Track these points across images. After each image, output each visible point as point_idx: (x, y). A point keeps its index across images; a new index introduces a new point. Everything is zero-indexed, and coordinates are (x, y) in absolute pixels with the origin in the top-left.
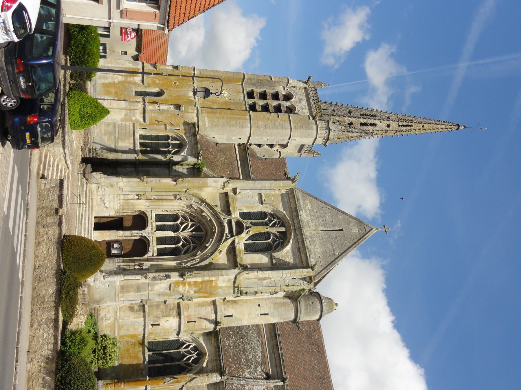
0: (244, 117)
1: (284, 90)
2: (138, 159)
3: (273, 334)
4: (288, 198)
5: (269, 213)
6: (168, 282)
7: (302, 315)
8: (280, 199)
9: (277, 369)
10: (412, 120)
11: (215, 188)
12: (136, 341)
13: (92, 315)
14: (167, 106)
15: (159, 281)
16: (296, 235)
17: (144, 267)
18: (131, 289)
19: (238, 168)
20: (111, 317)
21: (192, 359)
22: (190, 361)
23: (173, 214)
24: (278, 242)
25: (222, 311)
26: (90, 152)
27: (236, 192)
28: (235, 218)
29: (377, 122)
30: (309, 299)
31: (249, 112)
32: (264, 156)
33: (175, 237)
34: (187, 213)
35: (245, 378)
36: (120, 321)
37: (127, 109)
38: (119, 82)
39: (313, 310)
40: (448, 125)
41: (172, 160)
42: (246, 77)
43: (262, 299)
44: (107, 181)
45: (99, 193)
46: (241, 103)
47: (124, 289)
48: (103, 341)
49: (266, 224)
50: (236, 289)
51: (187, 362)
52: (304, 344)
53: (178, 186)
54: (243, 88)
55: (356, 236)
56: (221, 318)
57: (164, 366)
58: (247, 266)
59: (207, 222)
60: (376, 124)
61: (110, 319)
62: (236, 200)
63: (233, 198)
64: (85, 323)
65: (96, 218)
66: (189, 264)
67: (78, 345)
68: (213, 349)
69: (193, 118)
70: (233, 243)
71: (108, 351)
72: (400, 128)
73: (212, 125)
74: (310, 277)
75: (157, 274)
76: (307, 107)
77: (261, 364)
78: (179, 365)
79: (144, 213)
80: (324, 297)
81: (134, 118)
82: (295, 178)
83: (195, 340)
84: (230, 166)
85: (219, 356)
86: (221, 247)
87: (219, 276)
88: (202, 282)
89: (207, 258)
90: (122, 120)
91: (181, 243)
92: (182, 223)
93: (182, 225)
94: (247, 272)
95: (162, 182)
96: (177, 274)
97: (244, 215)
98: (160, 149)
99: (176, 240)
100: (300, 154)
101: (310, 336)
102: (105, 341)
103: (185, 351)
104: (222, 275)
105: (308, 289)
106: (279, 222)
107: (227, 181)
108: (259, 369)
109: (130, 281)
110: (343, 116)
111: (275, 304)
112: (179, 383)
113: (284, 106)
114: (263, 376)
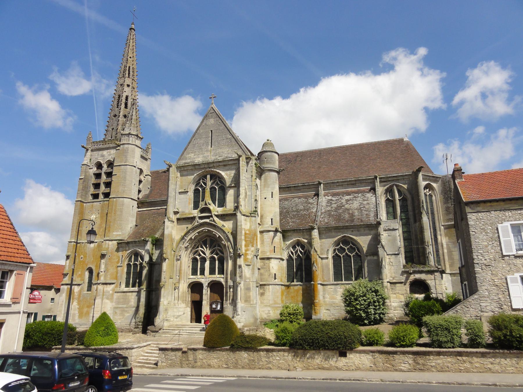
0: (114, 203)
1: (92, 168)
2: (146, 289)
3: (287, 189)
4: (184, 171)
5: (195, 187)
6: (244, 267)
7: (274, 167)
8: (184, 178)
9: (312, 188)
10: (125, 66)
11: (172, 228)
12: (286, 291)
13: (265, 323)
14: (102, 265)
15: (243, 273)
16: (214, 167)
17: (232, 284)
18: (248, 295)
19: (157, 209)
20: (268, 309)
21: (301, 250)
22: (303, 251)
23: (192, 262)
24: (218, 181)
25: (268, 227)
26: (138, 328)
27: (177, 212)
28: (198, 213)
29: (125, 95)
30: (262, 161)
31: (110, 198)
32: (149, 188)
33: (210, 261)
34: (191, 251)
35: (316, 212)
36: (271, 303)
37: (103, 297)
38: (79, 304)
39: (271, 158)
40: (130, 38)
41: (148, 261)
42: (80, 199)
43: (261, 196)
44: (162, 314)
45: (172, 319)
46: (102, 205)
47: (247, 300)
48: (284, 315)
49: (204, 190)
50: (252, 215)
51: (303, 254)
52: (296, 167)
53: (169, 257)
54: (89, 202)
55: (217, 120)
56: (273, 227)
57: (305, 271)
58: (235, 206)
59: (200, 235)
60: (126, 96)
61: (269, 311)
62: (183, 212)
63: (182, 215)
64: (271, 329)
65: (192, 322)
66: (231, 250)
67: (286, 333)
68: (295, 234)
69: (113, 244)
70: (217, 216)
71: (291, 312)
72: (131, 77)
73: (120, 229)
74: (247, 158)
75: (238, 275)
76: (108, 151)
77: (308, 199)
78: (305, 260)
79: (190, 285)
80: (262, 149)
81: (111, 292)
82: (168, 165)
83: (288, 248)
84: (155, 215)
85: (300, 230)
86: (220, 226)
87: (242, 228)
88: (245, 241)
89: (227, 236)
90: (112, 302)
91: (215, 256)
92: (200, 255)
93: (201, 255)
94: (240, 206)
95: (166, 270)
96: (238, 260)
97: (196, 207)
98: (138, 271)
99: (212, 260)
100: (149, 159)
101: (290, 162)
102: (285, 314)
103: (295, 255)
104: (241, 225)
105: (255, 161)
106: (203, 180)
107: (168, 218)
108: (311, 201)
110: (118, 122)
111: (265, 186)
112: (318, 259)
113: (107, 170)
114: (316, 199)
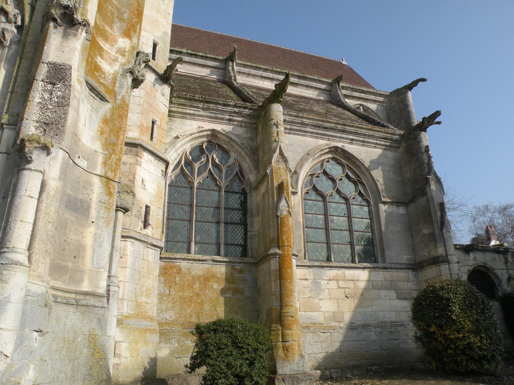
18: (72, 236)
109: (40, 224)
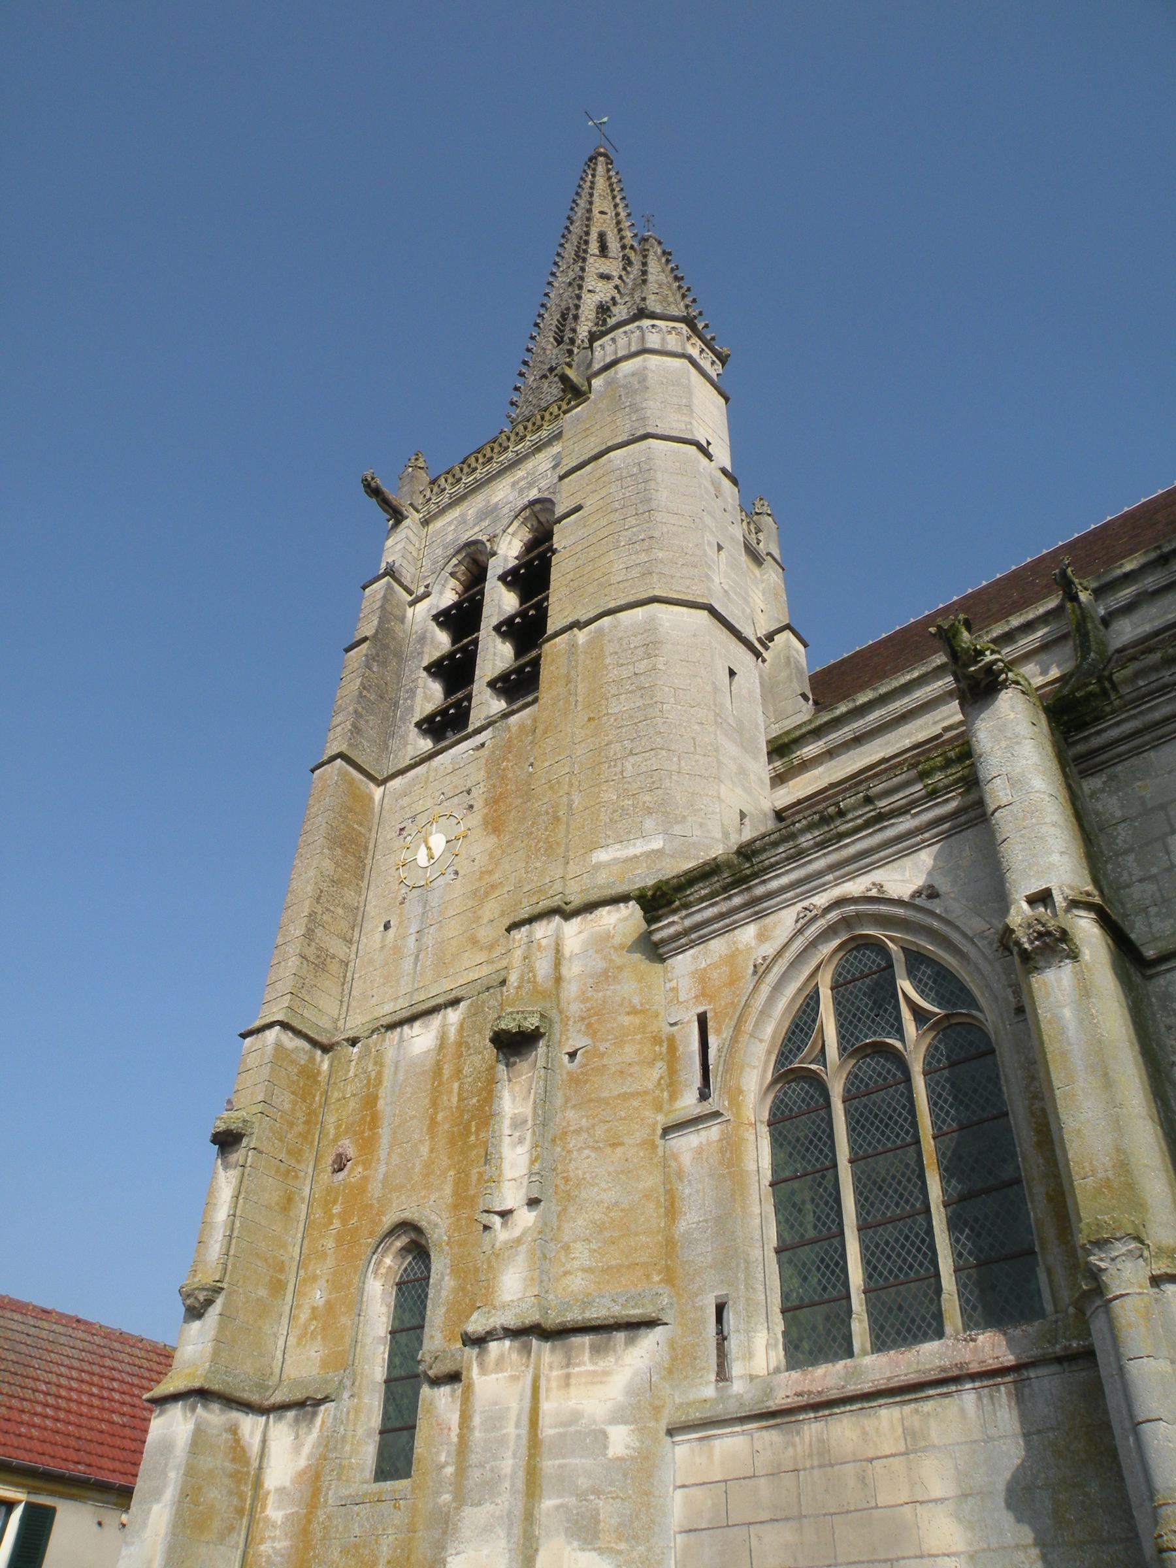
37: (529, 1517)
69: (601, 941)
73: (649, 811)
81: (620, 1440)
